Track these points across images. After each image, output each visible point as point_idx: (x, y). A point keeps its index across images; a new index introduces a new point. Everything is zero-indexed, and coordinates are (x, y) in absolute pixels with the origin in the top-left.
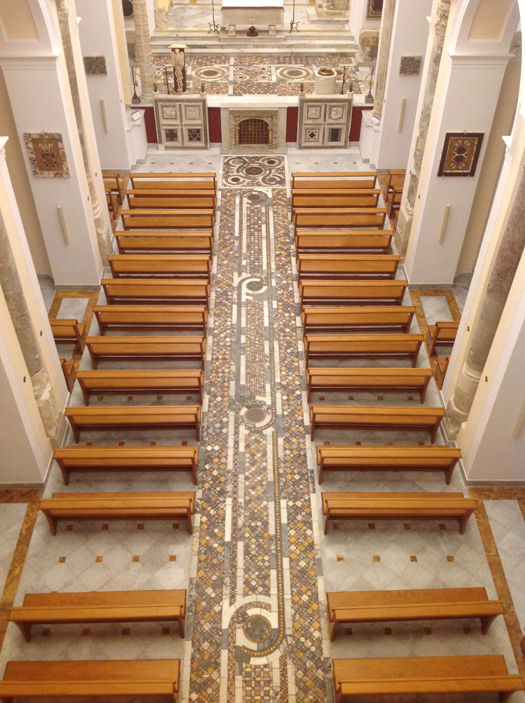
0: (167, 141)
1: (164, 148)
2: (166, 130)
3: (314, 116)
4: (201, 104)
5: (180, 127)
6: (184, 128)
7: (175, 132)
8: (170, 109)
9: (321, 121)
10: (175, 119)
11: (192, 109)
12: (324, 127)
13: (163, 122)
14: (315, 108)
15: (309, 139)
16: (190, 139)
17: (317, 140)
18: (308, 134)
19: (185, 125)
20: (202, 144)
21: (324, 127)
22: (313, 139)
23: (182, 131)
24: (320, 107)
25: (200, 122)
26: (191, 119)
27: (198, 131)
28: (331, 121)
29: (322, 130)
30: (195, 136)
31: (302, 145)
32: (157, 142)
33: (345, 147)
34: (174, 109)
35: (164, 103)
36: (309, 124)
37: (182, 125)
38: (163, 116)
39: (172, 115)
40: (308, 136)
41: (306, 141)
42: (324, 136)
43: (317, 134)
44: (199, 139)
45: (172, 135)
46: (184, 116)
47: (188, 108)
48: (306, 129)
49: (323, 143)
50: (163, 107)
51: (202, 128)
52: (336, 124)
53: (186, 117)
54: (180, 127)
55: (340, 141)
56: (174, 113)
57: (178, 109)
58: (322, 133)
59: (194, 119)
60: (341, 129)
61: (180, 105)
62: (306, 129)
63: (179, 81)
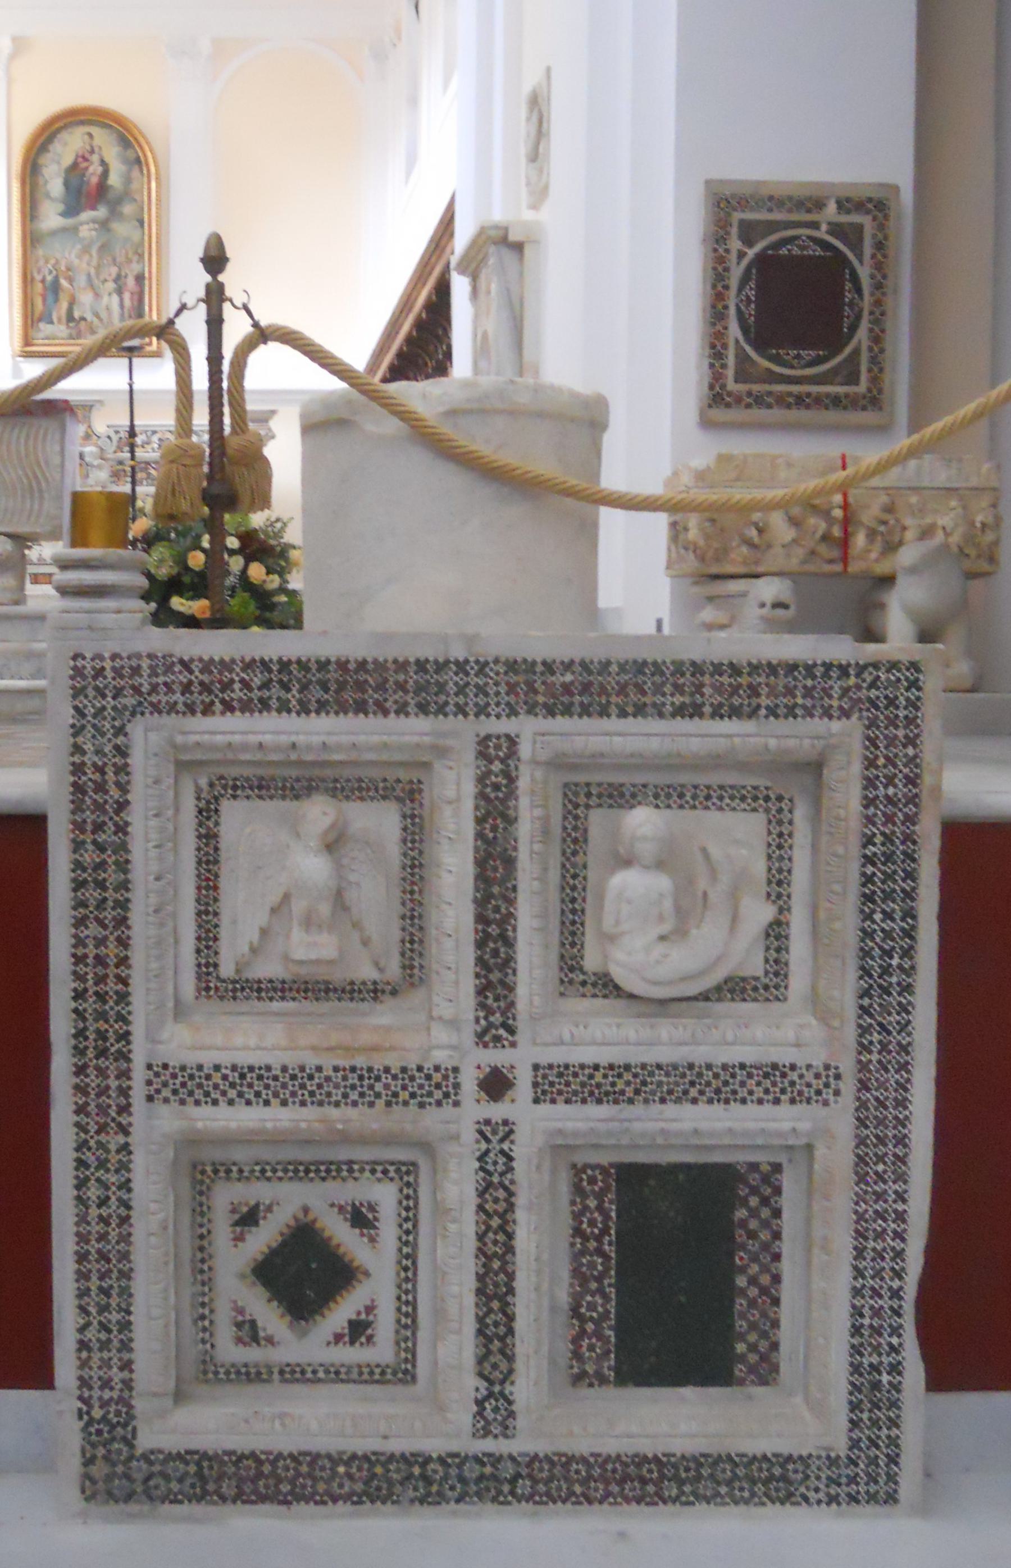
3: (308, 948)
9: (437, 1028)
12: (496, 1138)
14: (318, 813)
15: (249, 1332)
17: (382, 1351)
18: (235, 1258)
21: (496, 1138)
22: (315, 1344)
24: (405, 790)
28: (599, 1036)
29: (458, 1185)
31: (150, 1437)
33: (863, 1475)
36: (248, 1083)
40: (236, 1289)
41: (208, 1374)
42: (495, 1290)
43: (376, 1259)
48: (202, 1171)
49: (494, 1407)
52: (721, 1084)
55: (766, 1371)
58: (467, 1224)
60: (768, 1180)
62: (202, 1171)
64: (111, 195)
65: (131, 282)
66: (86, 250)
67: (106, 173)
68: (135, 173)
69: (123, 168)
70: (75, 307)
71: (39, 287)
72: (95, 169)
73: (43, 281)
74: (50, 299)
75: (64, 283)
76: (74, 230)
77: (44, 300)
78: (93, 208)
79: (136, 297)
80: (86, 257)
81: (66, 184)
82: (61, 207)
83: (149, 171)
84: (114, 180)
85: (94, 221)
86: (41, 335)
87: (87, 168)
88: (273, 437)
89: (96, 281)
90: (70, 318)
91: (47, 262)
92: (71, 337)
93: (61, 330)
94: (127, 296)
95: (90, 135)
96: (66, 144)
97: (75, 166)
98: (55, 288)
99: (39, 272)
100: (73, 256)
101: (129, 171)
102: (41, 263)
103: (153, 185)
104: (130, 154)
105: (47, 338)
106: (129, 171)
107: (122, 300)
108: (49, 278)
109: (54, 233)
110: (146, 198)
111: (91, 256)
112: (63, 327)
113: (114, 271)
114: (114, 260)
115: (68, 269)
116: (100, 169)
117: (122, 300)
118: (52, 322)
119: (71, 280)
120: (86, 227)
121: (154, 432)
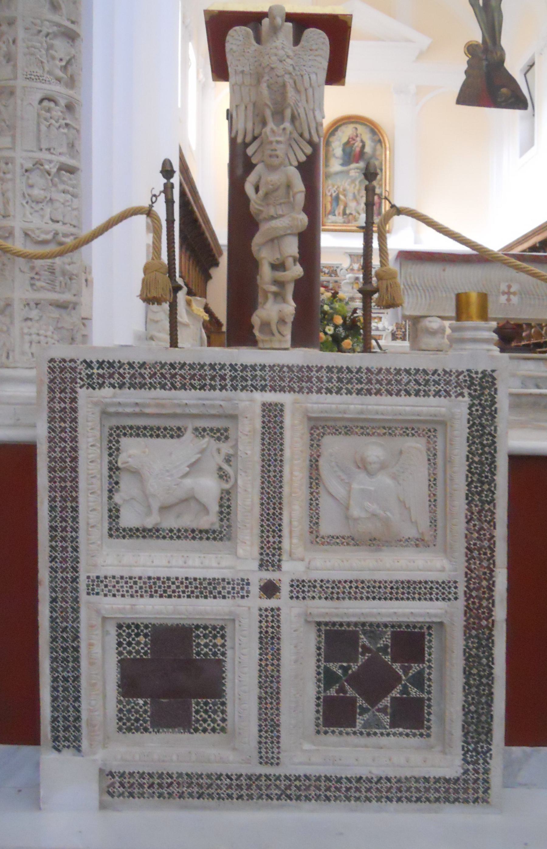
0: (128, 724)
1: (91, 791)
2: (127, 629)
4: (457, 409)
5: (256, 602)
6: (292, 614)
7: (202, 646)
8: (186, 448)
10: (218, 534)
11: (375, 450)
13: (103, 557)
16: (336, 714)
19: (301, 589)
20: (438, 758)
23: (270, 639)
25: (441, 565)
26: (352, 541)
27: (411, 642)
30: (374, 682)
32: (33, 739)
34: (215, 452)
35: (130, 397)
37: (270, 589)
38: (114, 513)
39: (190, 499)
44: (411, 716)
45: (173, 676)
46: (294, 512)
47: (334, 446)
50: (115, 436)
51: (450, 613)
53: (314, 521)
54: (256, 602)
56: (208, 486)
57: (250, 449)
59: (374, 543)
61: (273, 415)
63: (274, 240)
64: (366, 157)
66: (353, 181)
67: (363, 146)
68: (378, 147)
69: (373, 144)
70: (347, 209)
71: (329, 199)
72: (358, 145)
73: (331, 195)
74: (334, 204)
75: (342, 197)
76: (348, 172)
77: (331, 205)
78: (357, 162)
80: (353, 185)
81: (344, 150)
82: (341, 161)
83: (385, 146)
84: (368, 149)
85: (357, 168)
86: (329, 221)
87: (354, 144)
89: (358, 197)
90: (344, 213)
91: (333, 186)
92: (344, 222)
93: (340, 219)
95: (356, 129)
96: (343, 132)
97: (348, 143)
98: (337, 199)
99: (329, 191)
100: (346, 184)
101: (375, 146)
102: (330, 187)
103: (388, 153)
104: (376, 138)
105: (333, 222)
106: (375, 146)
108: (334, 195)
109: (337, 173)
110: (384, 158)
111: (356, 185)
112: (341, 218)
116: (361, 144)
118: (335, 215)
119: (345, 196)
120: (353, 171)
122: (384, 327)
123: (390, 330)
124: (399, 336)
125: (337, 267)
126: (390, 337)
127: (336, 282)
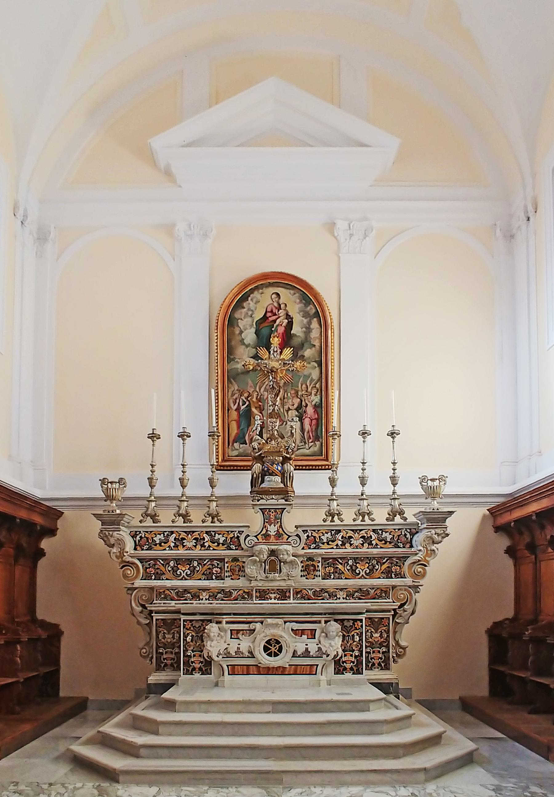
65: (310, 410)
71: (234, 415)
79: (314, 422)
88: (447, 535)
94: (307, 422)
107: (302, 424)
108: (243, 408)
113: (297, 401)
114: (297, 392)
115: (259, 400)
117: (302, 424)
121: (339, 531)
122: (320, 649)
123: (330, 658)
124: (348, 666)
125: (241, 532)
126: (331, 668)
127: (235, 559)
